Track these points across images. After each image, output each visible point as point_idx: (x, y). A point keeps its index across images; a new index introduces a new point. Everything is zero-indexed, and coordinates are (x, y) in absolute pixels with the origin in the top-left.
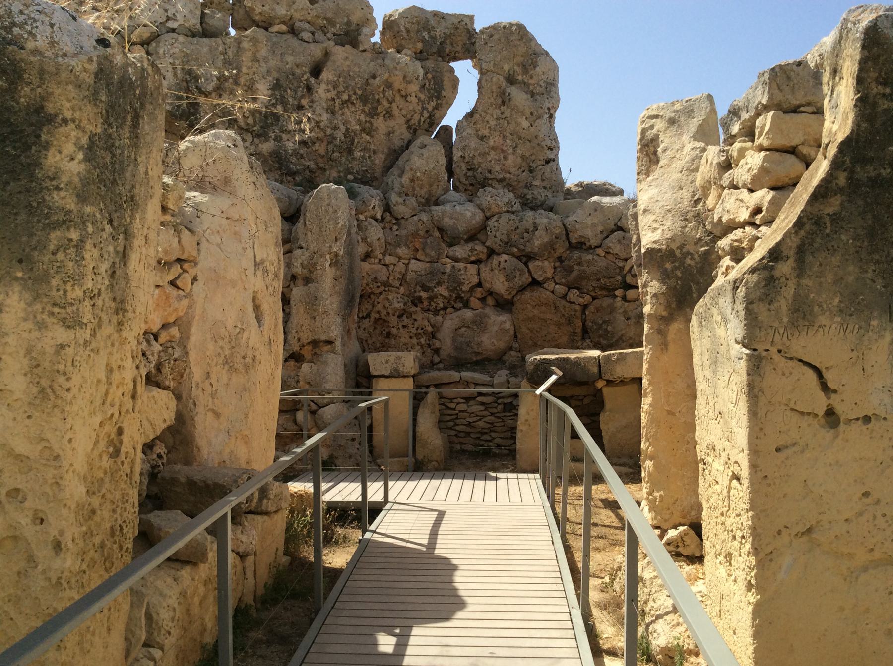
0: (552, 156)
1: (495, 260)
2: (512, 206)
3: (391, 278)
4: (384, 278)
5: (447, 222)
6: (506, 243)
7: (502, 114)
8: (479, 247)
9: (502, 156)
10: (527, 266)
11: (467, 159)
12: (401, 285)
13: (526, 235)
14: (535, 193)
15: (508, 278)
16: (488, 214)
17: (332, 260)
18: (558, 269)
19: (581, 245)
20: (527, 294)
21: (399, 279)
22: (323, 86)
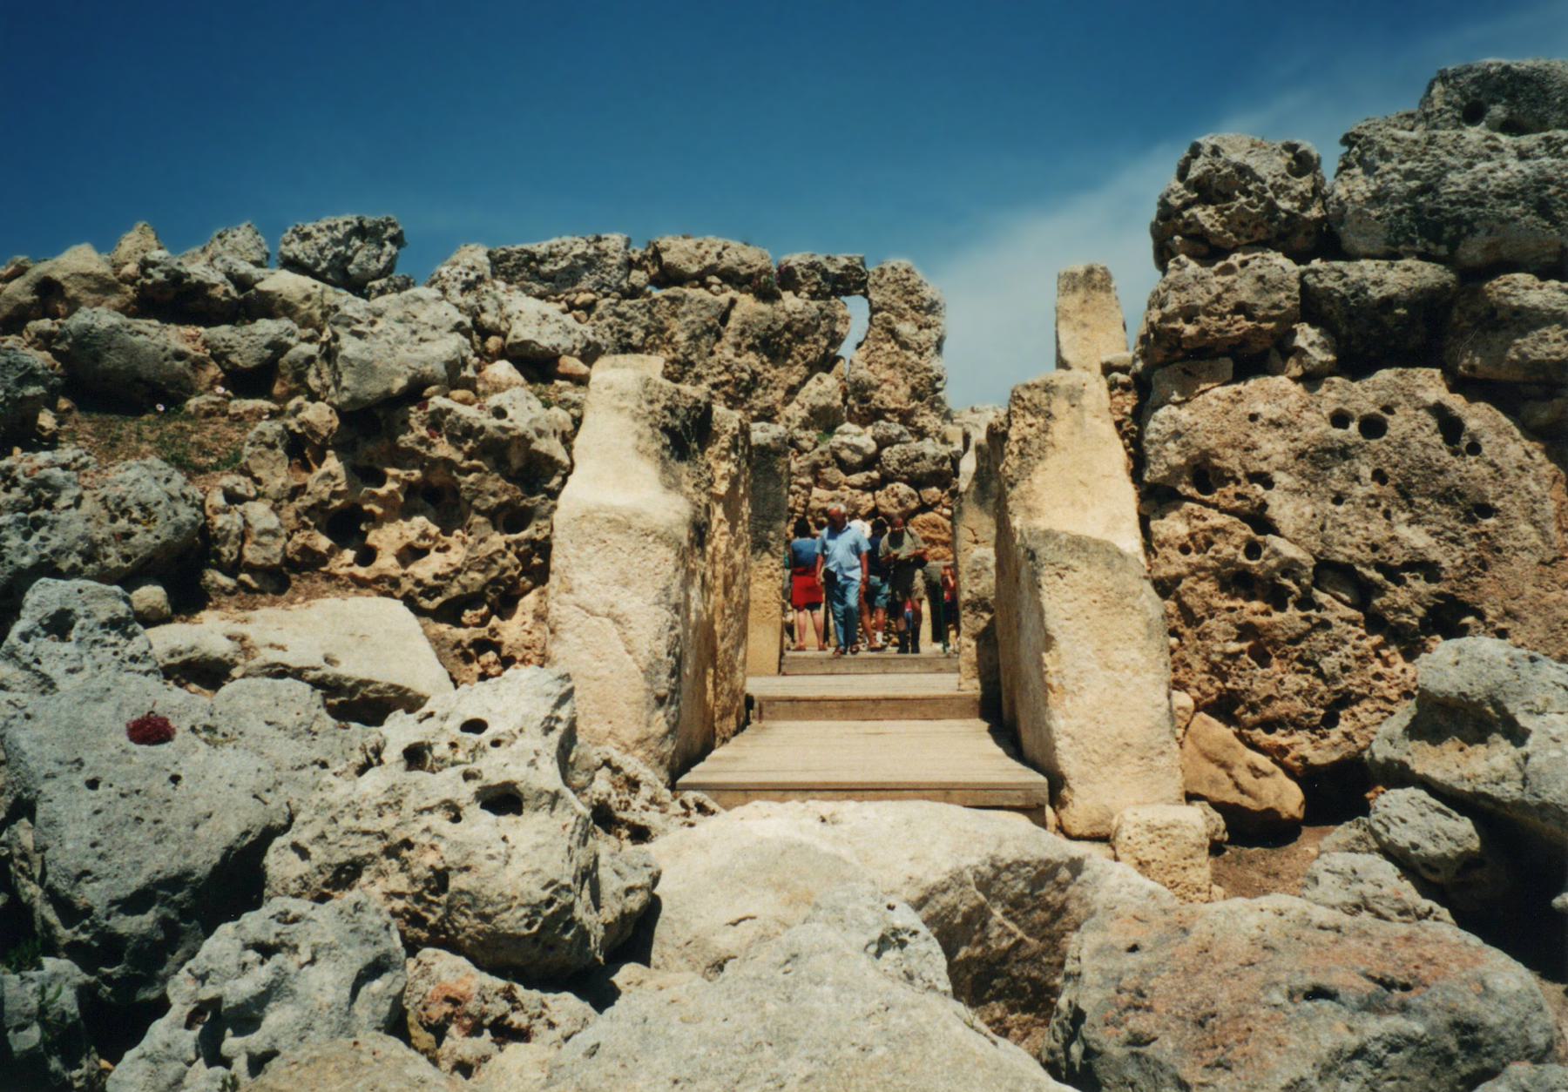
8: (875, 474)
15: (901, 503)
20: (920, 518)
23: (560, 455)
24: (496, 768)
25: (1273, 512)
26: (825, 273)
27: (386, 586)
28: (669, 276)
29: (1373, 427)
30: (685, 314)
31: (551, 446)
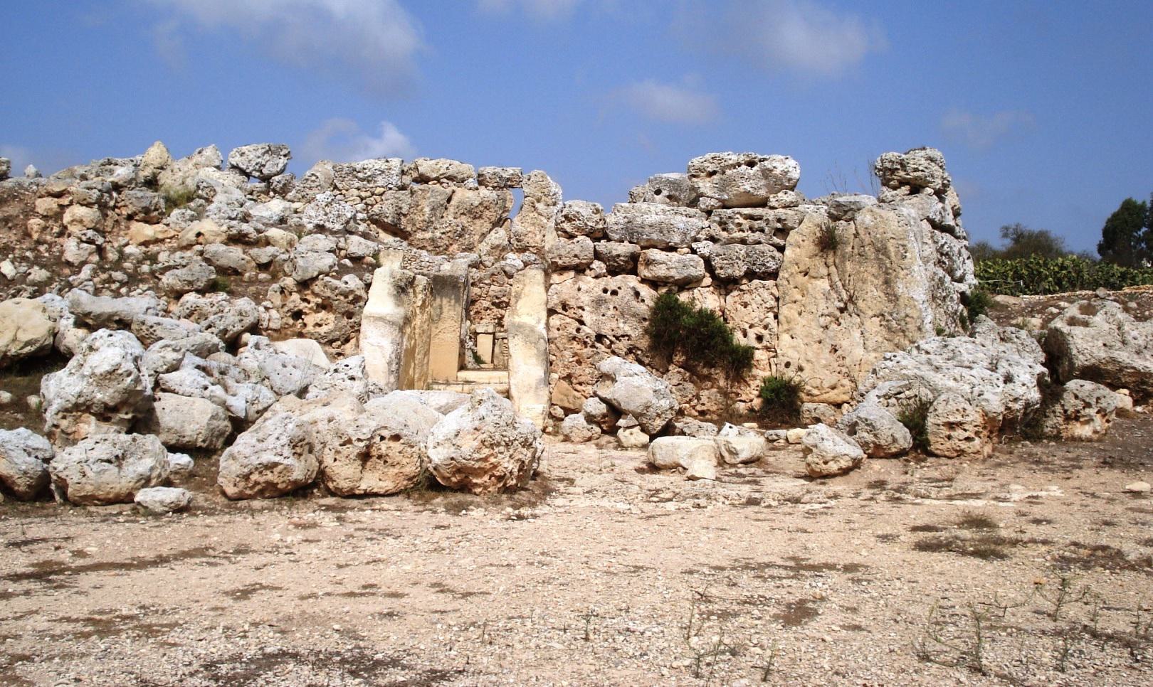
23: (364, 295)
24: (351, 373)
25: (584, 319)
26: (501, 177)
27: (311, 336)
28: (423, 179)
29: (614, 293)
31: (361, 293)
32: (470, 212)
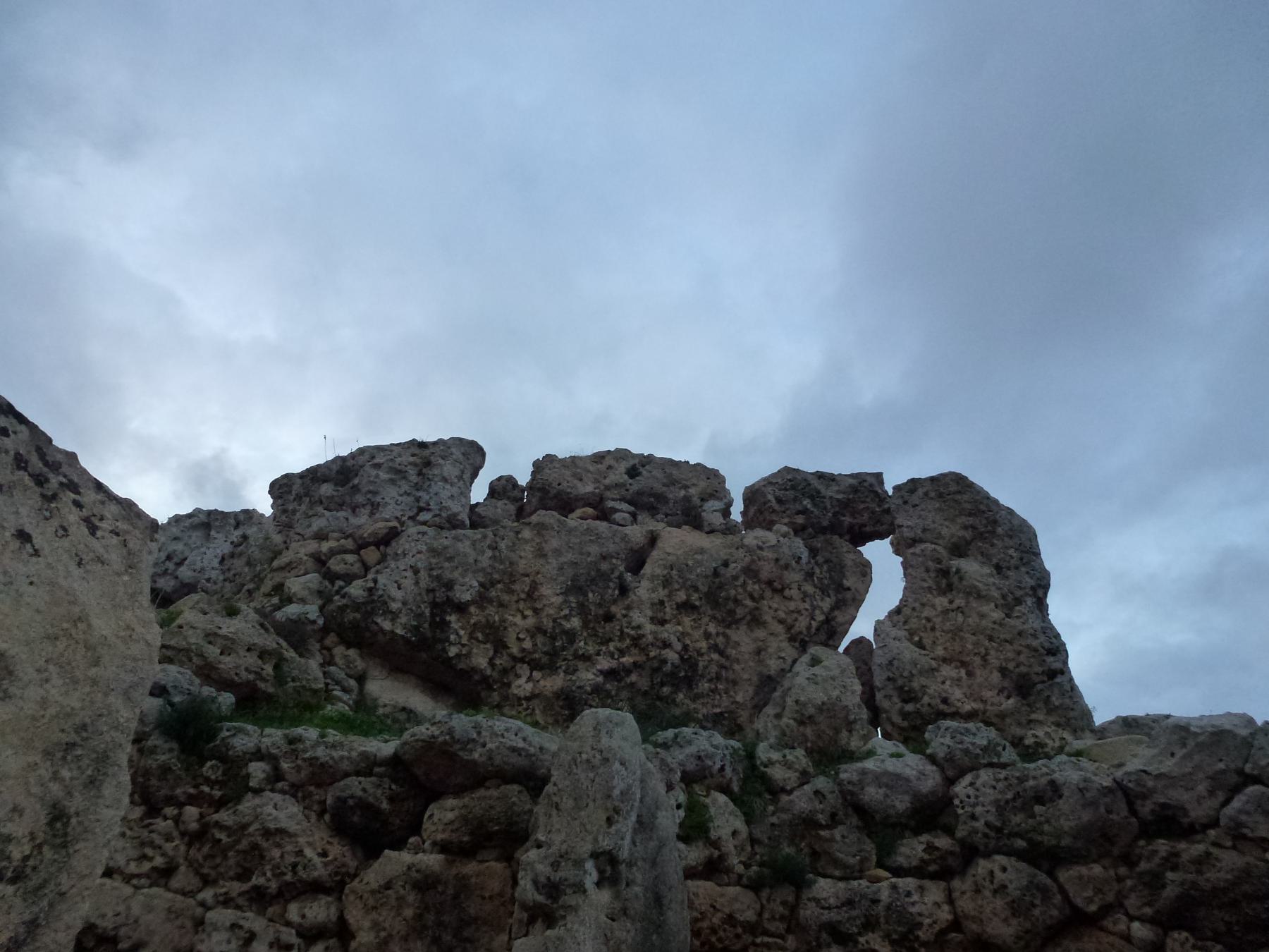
0: (1058, 665)
1: (982, 866)
2: (999, 755)
3: (766, 915)
4: (750, 915)
5: (872, 794)
6: (999, 830)
7: (951, 602)
8: (943, 842)
9: (963, 672)
10: (1055, 880)
11: (900, 682)
12: (788, 931)
13: (1038, 809)
14: (1041, 733)
15: (1016, 908)
16: (950, 773)
17: (601, 872)
18: (1129, 883)
19: (1170, 823)
21: (782, 918)
22: (645, 584)
30: (558, 552)
32: (712, 598)
